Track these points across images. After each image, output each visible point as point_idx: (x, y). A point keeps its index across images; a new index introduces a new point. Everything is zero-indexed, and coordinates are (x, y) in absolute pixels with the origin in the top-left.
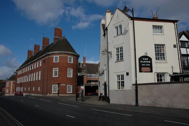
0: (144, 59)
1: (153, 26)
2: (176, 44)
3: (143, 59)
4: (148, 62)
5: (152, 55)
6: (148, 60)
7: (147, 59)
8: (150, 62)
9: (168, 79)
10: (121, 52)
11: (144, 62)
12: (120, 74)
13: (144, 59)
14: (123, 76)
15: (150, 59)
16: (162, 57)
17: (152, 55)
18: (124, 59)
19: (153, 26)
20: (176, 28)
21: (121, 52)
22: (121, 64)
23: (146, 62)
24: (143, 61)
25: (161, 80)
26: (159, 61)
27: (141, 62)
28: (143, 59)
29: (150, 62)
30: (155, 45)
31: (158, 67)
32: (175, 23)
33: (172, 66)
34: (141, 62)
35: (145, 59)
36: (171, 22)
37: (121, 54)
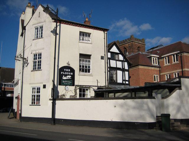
0: (66, 70)
1: (81, 32)
2: (104, 56)
3: (65, 70)
5: (75, 66)
6: (70, 72)
7: (69, 70)
8: (72, 74)
9: (90, 93)
10: (39, 60)
11: (66, 73)
12: (36, 86)
13: (66, 70)
14: (39, 89)
15: (73, 71)
18: (41, 69)
19: (81, 32)
20: (107, 38)
21: (39, 60)
22: (37, 73)
23: (67, 73)
24: (65, 72)
25: (84, 95)
26: (83, 73)
27: (62, 73)
28: (65, 70)
29: (72, 74)
31: (81, 79)
32: (105, 32)
33: (97, 80)
34: (62, 73)
35: (67, 70)
36: (101, 31)
37: (38, 61)
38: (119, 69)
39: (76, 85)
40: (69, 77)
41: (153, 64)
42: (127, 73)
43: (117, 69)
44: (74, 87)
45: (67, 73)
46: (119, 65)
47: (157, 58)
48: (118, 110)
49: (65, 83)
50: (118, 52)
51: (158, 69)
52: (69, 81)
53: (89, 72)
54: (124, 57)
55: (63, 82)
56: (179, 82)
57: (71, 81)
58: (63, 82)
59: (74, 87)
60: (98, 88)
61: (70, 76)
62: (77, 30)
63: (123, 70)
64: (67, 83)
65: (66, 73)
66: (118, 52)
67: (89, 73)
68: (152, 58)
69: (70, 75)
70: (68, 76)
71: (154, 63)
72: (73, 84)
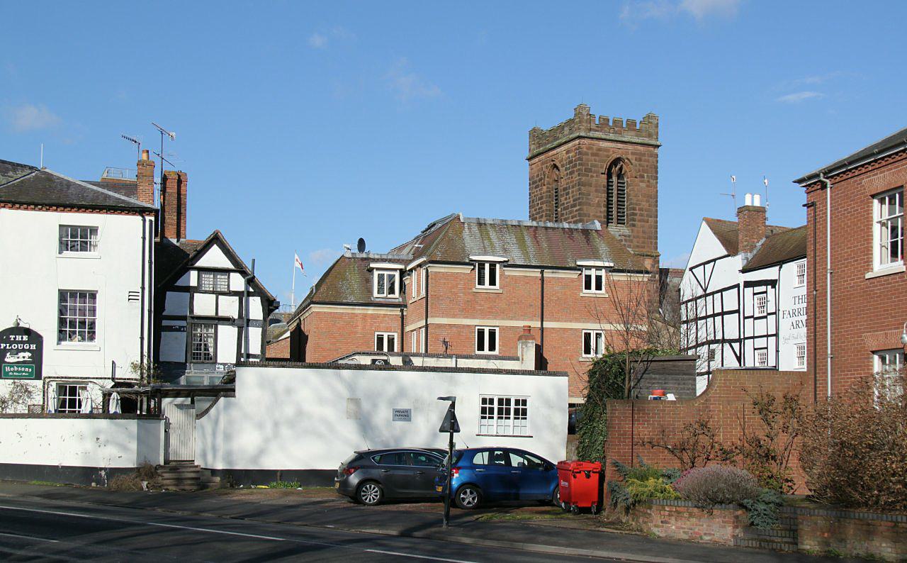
0: (15, 338)
2: (140, 290)
4: (26, 346)
5: (47, 327)
6: (29, 342)
7: (25, 338)
9: (91, 397)
13: (15, 338)
15: (35, 338)
16: (77, 330)
17: (47, 327)
24: (15, 342)
29: (33, 347)
30: (63, 295)
32: (148, 218)
33: (113, 362)
35: (19, 338)
38: (227, 320)
39: (45, 378)
40: (24, 357)
41: (375, 294)
42: (255, 334)
43: (217, 320)
44: (41, 382)
45: (20, 346)
46: (229, 307)
47: (397, 274)
48: (89, 445)
49: (13, 372)
50: (231, 266)
51: (397, 311)
52: (25, 367)
53: (92, 338)
54: (251, 281)
55: (8, 369)
56: (231, 379)
57: (32, 367)
58: (8, 369)
59: (41, 382)
60: (117, 385)
61: (28, 354)
62: (50, 222)
63: (243, 323)
64: (18, 371)
65: (15, 346)
66: (231, 266)
67: (90, 343)
68: (376, 273)
69: (29, 350)
70: (21, 354)
71: (380, 291)
72: (38, 376)
